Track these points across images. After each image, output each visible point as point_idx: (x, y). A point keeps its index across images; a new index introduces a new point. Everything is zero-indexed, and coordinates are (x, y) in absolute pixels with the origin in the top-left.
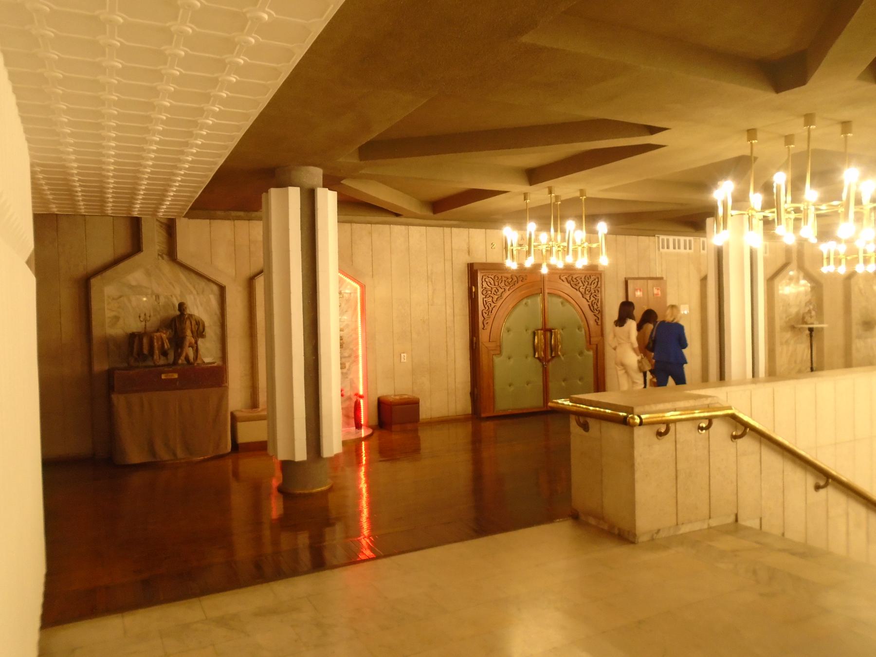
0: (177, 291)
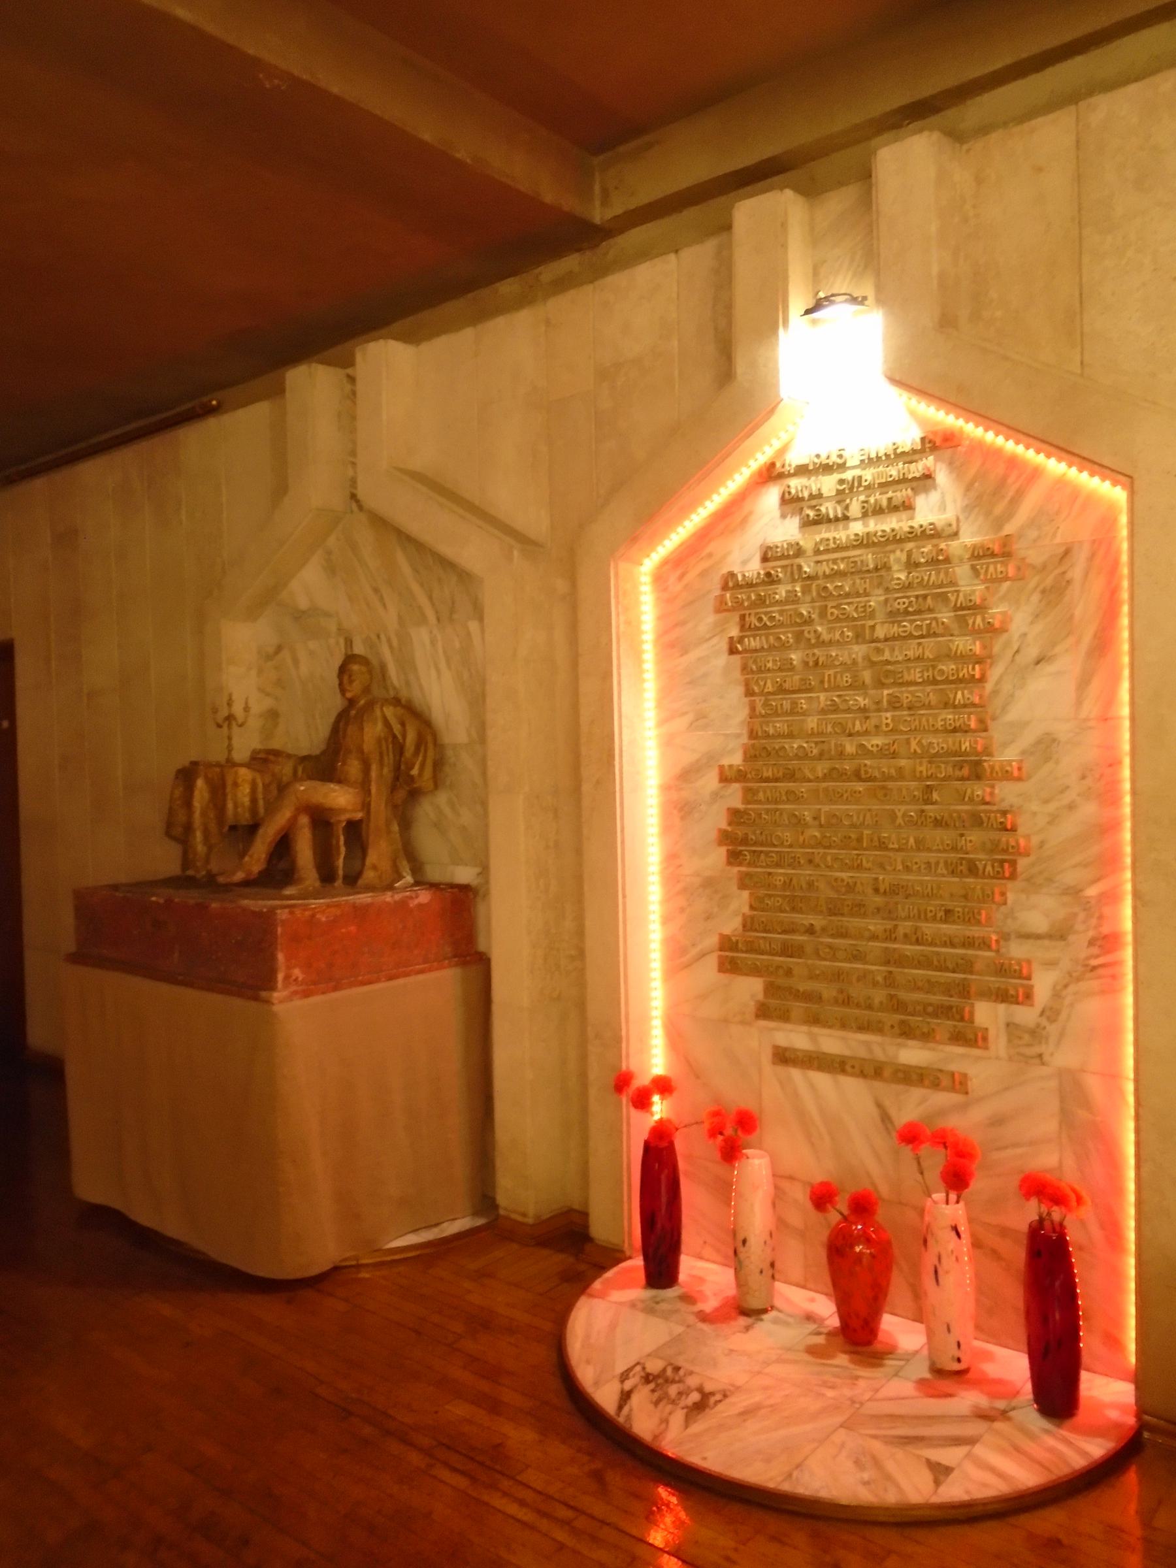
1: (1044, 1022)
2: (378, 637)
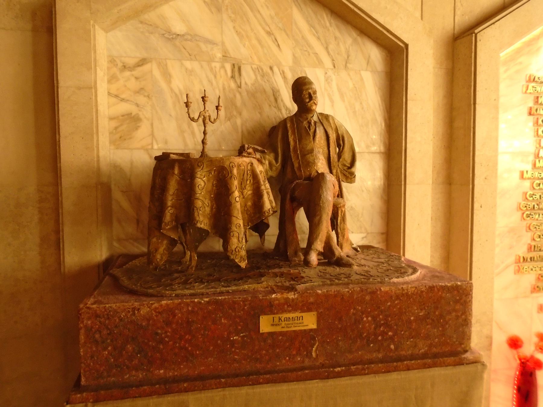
2: (271, 68)
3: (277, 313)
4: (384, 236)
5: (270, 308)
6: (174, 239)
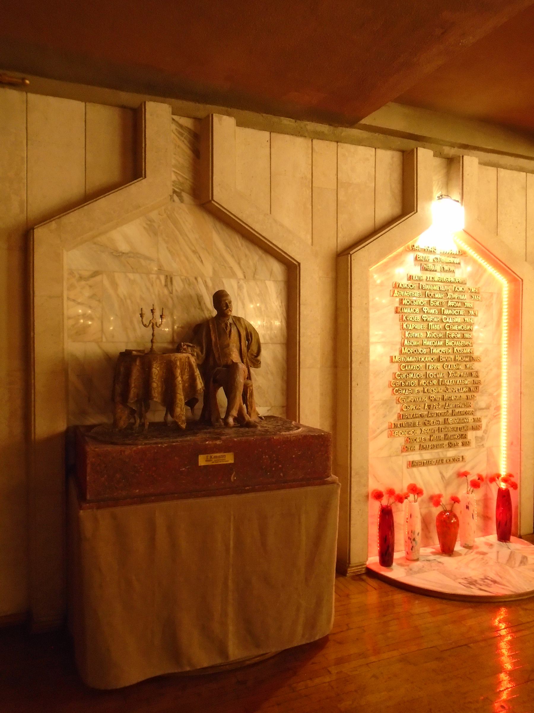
0: (208, 269)
1: (484, 434)
2: (196, 279)
3: (209, 453)
4: (285, 409)
5: (206, 450)
6: (134, 410)
